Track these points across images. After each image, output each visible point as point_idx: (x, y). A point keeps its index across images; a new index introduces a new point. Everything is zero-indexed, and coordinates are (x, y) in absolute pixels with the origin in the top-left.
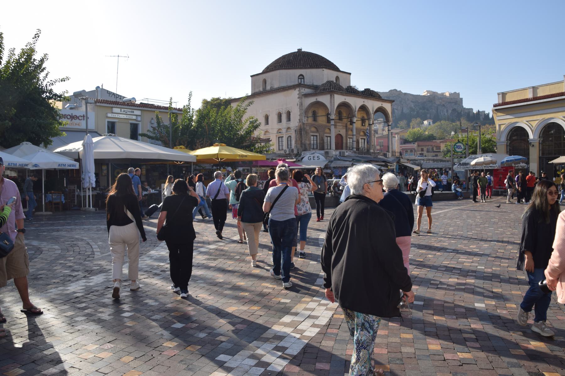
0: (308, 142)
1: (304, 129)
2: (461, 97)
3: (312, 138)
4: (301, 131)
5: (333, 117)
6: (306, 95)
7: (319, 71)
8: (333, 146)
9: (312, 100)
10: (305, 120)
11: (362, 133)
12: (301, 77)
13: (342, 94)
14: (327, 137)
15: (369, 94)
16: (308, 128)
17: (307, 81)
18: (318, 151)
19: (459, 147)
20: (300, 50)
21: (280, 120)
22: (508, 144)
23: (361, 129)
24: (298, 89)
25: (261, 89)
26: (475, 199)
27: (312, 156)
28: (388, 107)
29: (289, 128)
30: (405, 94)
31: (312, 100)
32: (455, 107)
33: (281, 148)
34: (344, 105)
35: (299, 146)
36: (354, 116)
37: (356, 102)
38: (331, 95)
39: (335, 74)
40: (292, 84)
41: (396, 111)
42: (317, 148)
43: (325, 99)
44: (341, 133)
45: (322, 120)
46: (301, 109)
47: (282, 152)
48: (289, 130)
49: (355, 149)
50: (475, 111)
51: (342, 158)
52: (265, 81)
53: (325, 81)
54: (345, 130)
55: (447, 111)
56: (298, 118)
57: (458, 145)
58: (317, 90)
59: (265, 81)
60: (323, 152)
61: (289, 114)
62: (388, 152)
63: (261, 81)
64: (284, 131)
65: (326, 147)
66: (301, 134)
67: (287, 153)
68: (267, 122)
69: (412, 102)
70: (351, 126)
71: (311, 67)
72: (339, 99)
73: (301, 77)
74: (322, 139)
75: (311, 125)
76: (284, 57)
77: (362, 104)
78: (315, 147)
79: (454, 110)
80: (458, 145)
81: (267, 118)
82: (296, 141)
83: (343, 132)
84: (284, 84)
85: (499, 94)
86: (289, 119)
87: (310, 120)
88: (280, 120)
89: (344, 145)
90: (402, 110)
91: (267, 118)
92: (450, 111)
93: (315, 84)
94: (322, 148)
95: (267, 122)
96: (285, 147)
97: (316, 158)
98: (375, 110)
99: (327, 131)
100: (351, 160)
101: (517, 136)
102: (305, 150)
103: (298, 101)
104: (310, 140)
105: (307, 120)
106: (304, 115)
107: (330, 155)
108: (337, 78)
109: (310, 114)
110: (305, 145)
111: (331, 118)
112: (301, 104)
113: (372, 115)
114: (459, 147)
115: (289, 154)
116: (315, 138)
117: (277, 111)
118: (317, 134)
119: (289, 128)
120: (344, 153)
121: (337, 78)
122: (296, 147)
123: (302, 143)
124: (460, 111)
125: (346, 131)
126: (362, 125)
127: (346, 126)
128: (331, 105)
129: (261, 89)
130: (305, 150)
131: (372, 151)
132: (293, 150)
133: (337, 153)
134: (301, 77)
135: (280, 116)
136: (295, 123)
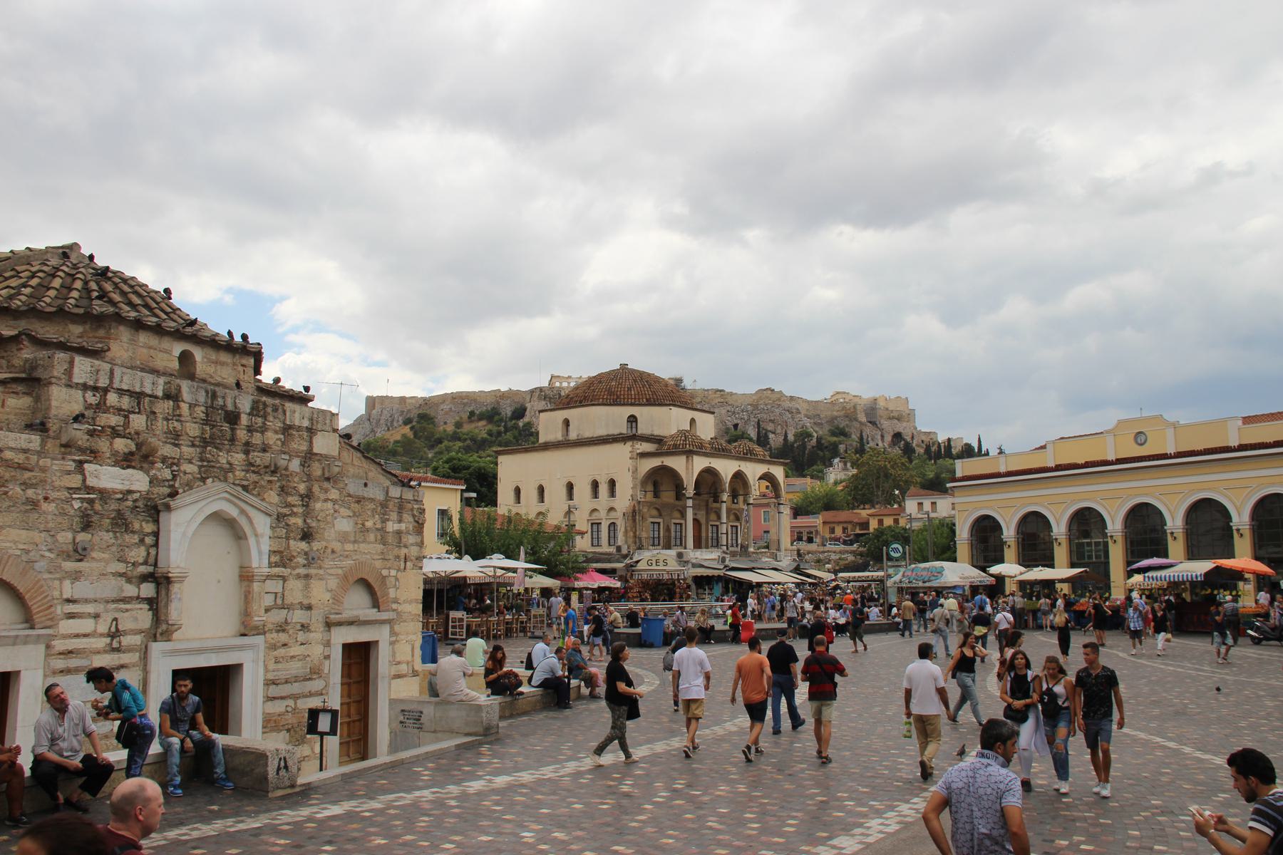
0: (644, 535)
4: (634, 515)
6: (644, 455)
10: (640, 496)
11: (732, 517)
13: (706, 455)
16: (645, 510)
17: (643, 429)
20: (624, 366)
26: (903, 635)
29: (612, 509)
31: (655, 462)
32: (900, 427)
33: (595, 542)
34: (709, 472)
35: (630, 541)
37: (726, 468)
40: (616, 431)
41: (771, 436)
44: (699, 517)
45: (668, 496)
48: (613, 514)
50: (941, 438)
52: (567, 423)
53: (674, 431)
54: (704, 512)
55: (882, 436)
56: (631, 492)
58: (662, 445)
59: (567, 423)
60: (672, 553)
61: (612, 483)
63: (560, 422)
64: (603, 514)
65: (673, 543)
66: (634, 521)
70: (715, 505)
71: (651, 403)
72: (700, 463)
73: (632, 420)
74: (668, 530)
75: (650, 505)
76: (600, 379)
79: (898, 436)
81: (570, 487)
82: (626, 531)
83: (702, 517)
84: (601, 432)
86: (612, 493)
87: (650, 496)
91: (570, 487)
92: (888, 438)
93: (656, 433)
97: (661, 563)
99: (677, 514)
101: (986, 529)
102: (640, 548)
103: (630, 463)
106: (639, 487)
108: (693, 421)
109: (650, 487)
112: (635, 471)
114: (896, 550)
117: (590, 480)
118: (660, 520)
121: (693, 421)
123: (635, 536)
124: (909, 439)
125: (707, 513)
127: (707, 505)
129: (559, 436)
132: (619, 549)
134: (632, 420)
135: (595, 485)
136: (623, 501)
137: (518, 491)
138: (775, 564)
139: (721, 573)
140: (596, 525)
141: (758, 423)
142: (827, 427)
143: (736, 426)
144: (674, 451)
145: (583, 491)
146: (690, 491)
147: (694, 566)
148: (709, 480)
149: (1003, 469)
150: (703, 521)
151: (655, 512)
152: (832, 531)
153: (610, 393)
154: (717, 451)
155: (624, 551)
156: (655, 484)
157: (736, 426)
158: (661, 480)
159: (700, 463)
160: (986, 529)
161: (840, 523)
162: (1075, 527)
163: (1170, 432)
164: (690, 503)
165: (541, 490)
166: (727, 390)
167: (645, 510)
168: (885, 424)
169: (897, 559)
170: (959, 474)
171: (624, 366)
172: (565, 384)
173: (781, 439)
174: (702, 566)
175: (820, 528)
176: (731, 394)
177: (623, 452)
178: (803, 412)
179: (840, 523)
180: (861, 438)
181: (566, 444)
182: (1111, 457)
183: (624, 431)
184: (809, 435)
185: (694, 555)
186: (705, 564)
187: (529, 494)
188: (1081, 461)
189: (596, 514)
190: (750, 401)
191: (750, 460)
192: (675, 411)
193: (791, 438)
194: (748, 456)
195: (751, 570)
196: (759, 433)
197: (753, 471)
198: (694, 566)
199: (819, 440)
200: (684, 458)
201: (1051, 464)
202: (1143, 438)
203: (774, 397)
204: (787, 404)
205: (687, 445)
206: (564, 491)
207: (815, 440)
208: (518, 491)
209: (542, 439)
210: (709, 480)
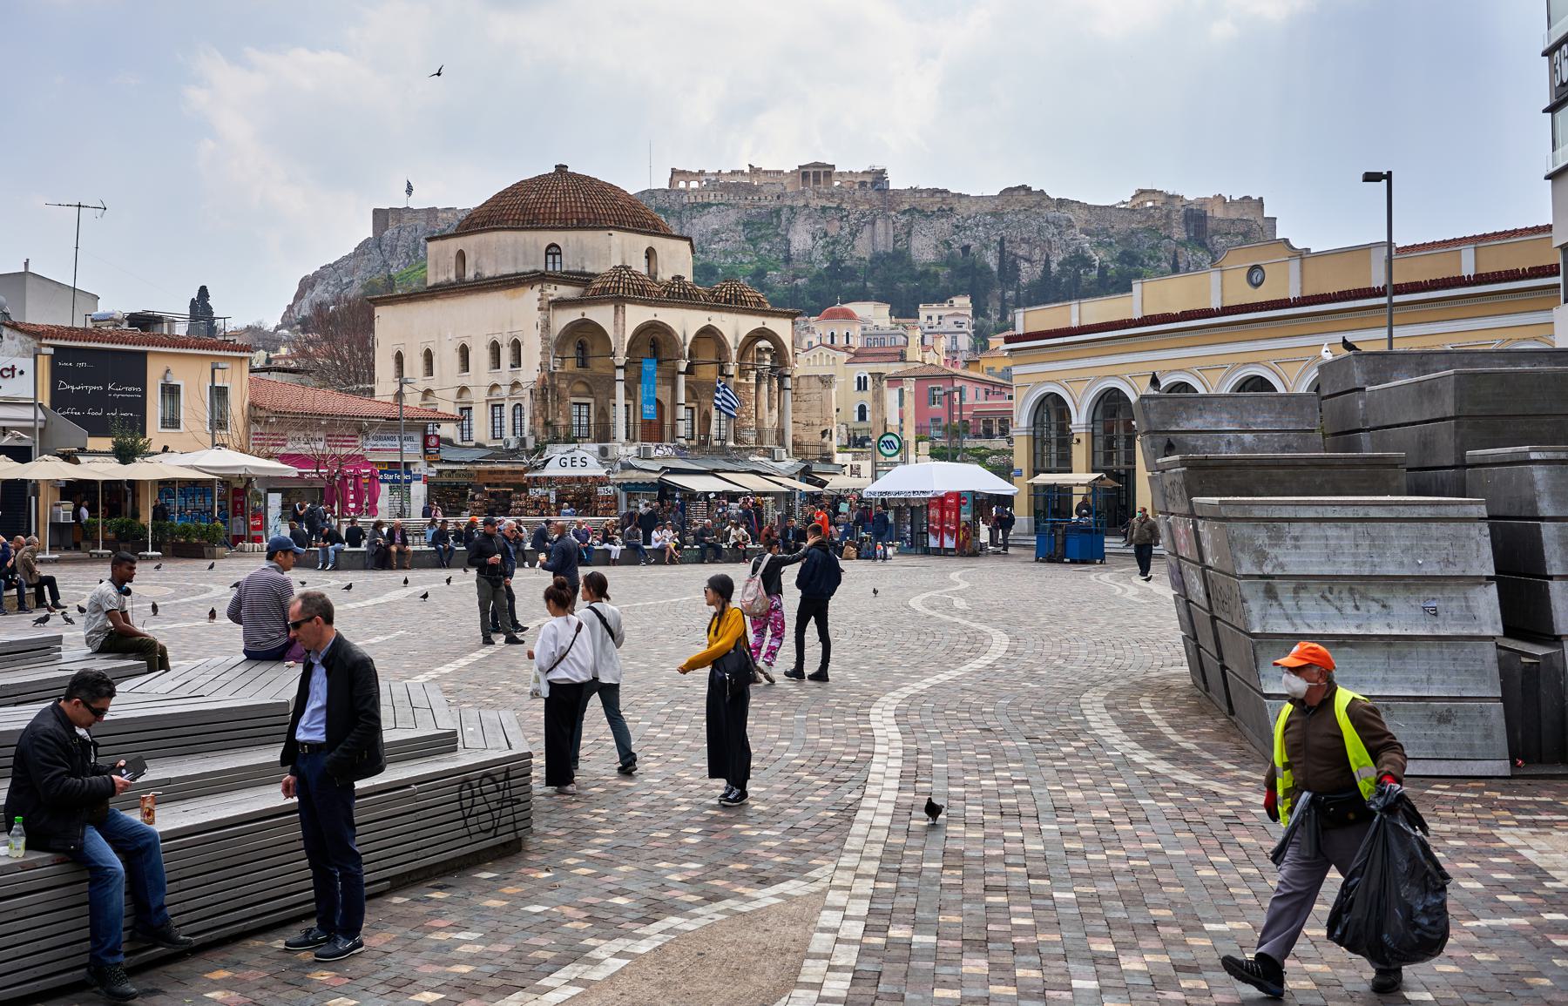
0: (562, 421)
1: (554, 387)
3: (575, 409)
4: (546, 392)
6: (560, 304)
7: (602, 234)
8: (620, 432)
9: (574, 315)
12: (554, 250)
16: (563, 385)
17: (569, 263)
18: (583, 447)
20: (561, 168)
21: (496, 363)
24: (538, 287)
25: (452, 277)
27: (569, 456)
29: (516, 385)
30: (1061, 203)
31: (574, 315)
33: (497, 434)
35: (539, 430)
36: (681, 356)
37: (685, 323)
39: (645, 241)
41: (1024, 265)
43: (602, 315)
46: (545, 339)
47: (500, 443)
51: (639, 463)
52: (461, 256)
56: (539, 359)
59: (461, 256)
60: (595, 447)
61: (516, 346)
63: (453, 254)
64: (505, 391)
66: (545, 401)
67: (511, 447)
68: (465, 365)
69: (1083, 231)
71: (581, 226)
72: (638, 315)
73: (553, 250)
75: (572, 378)
78: (584, 432)
81: (464, 352)
82: (533, 419)
84: (508, 269)
86: (517, 362)
87: (570, 365)
88: (496, 363)
89: (667, 430)
90: (1048, 263)
91: (464, 352)
93: (588, 270)
94: (598, 440)
95: (465, 365)
96: (508, 433)
97: (579, 463)
98: (741, 339)
103: (538, 316)
104: (569, 416)
105: (562, 365)
108: (650, 254)
109: (571, 351)
110: (555, 428)
112: (547, 326)
113: (734, 354)
115: (517, 450)
116: (584, 409)
119: (516, 385)
120: (647, 450)
121: (650, 254)
122: (533, 432)
123: (547, 424)
129: (452, 277)
130: (556, 440)
132: (523, 441)
133: (633, 449)
134: (553, 250)
135: (495, 349)
136: (530, 373)
137: (399, 358)
140: (496, 407)
141: (1001, 243)
143: (966, 249)
145: (480, 356)
146: (621, 359)
148: (653, 340)
149: (1075, 323)
150: (667, 402)
151: (580, 388)
153: (525, 210)
154: (677, 295)
155: (530, 445)
156: (582, 348)
157: (966, 249)
158: (583, 342)
163: (1295, 264)
164: (620, 374)
165: (428, 356)
167: (563, 385)
170: (1020, 331)
171: (561, 168)
172: (694, 185)
173: (1039, 269)
177: (530, 297)
181: (460, 287)
182: (1215, 304)
183: (542, 268)
187: (414, 365)
188: (1177, 310)
189: (497, 391)
190: (989, 207)
191: (730, 310)
192: (617, 236)
193: (1054, 267)
194: (734, 303)
195: (713, 473)
197: (734, 327)
201: (1137, 316)
202: (1256, 276)
203: (1031, 200)
204: (1051, 213)
205: (623, 288)
206: (456, 358)
208: (399, 358)
209: (430, 282)
210: (653, 340)
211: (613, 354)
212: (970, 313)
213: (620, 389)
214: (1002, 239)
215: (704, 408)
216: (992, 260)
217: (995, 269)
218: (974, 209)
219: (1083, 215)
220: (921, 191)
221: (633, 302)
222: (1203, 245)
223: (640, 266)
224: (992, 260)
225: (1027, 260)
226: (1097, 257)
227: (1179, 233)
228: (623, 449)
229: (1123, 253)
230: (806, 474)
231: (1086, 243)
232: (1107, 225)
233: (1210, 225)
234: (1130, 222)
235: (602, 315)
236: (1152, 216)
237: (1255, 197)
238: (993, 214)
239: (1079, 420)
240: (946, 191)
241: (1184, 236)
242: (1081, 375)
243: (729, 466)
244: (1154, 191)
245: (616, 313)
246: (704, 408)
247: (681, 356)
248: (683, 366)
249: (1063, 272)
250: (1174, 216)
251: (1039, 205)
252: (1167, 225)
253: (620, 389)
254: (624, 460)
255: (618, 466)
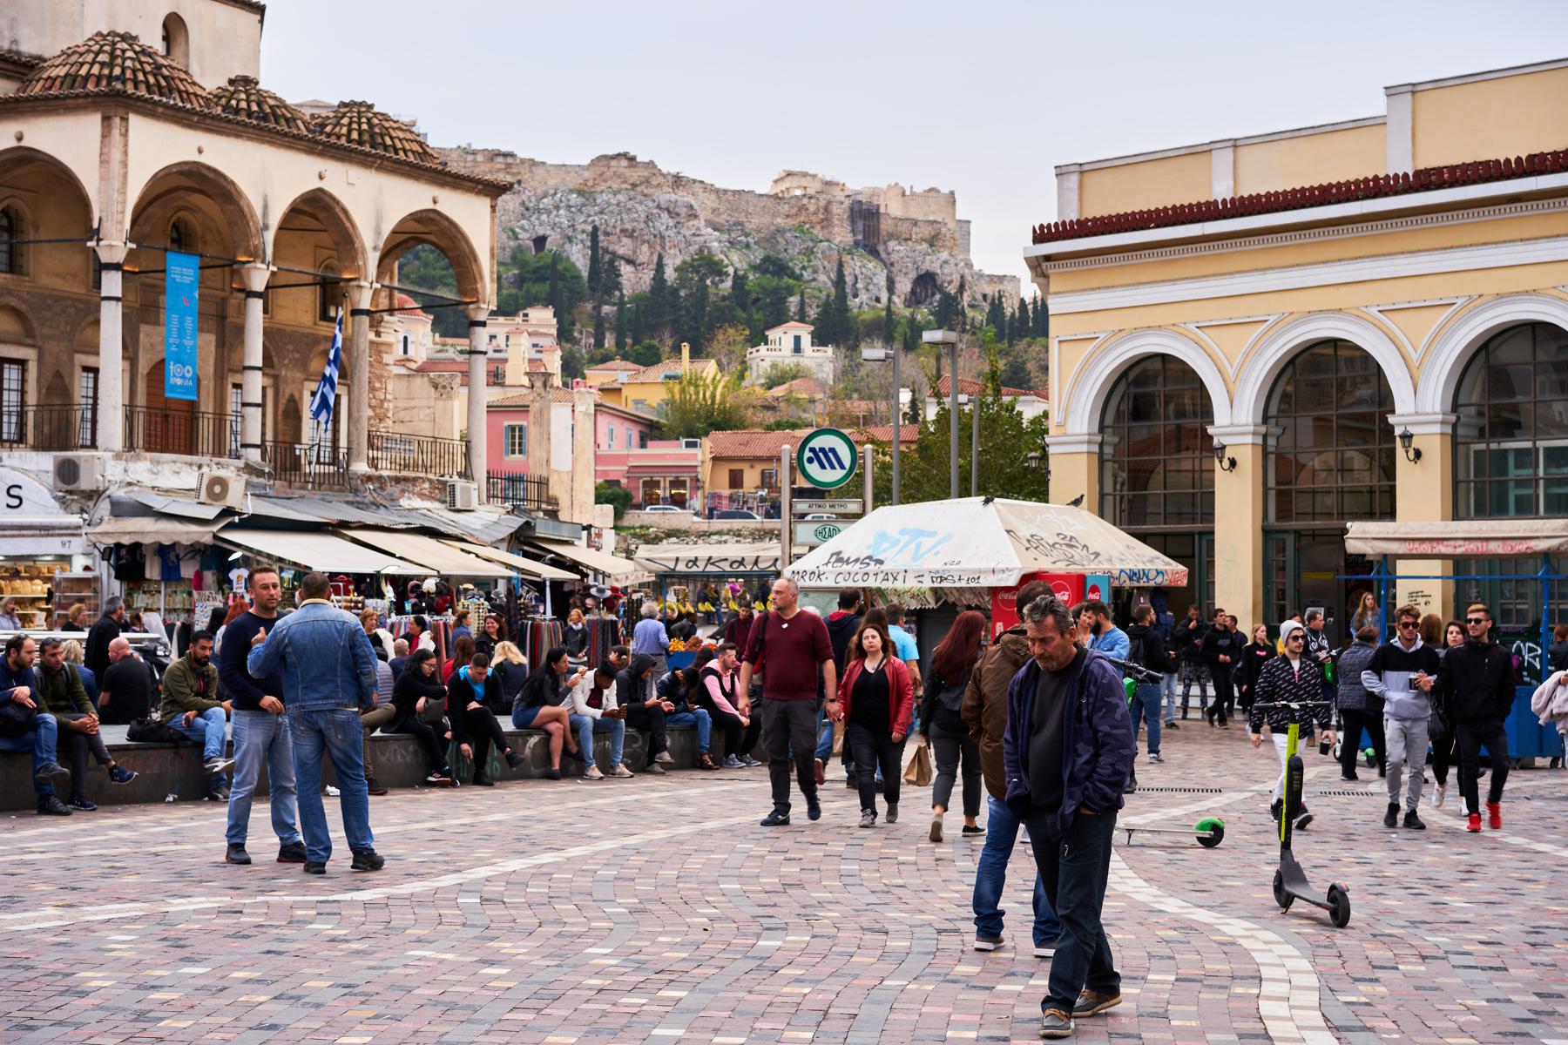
2: (961, 214)
5: (115, 244)
14: (86, 369)
15: (364, 138)
19: (826, 457)
22: (1108, 450)
23: (315, 340)
28: (472, 218)
30: (678, 181)
32: (931, 263)
36: (257, 254)
37: (269, 179)
38: (106, 119)
41: (626, 270)
42: (21, 439)
43: (68, 140)
49: (254, 455)
53: (81, 35)
57: (816, 443)
60: (46, 461)
62: (466, 475)
69: (709, 223)
72: (155, 146)
74: (57, 389)
77: (317, 184)
79: (926, 282)
80: (816, 443)
85: (1061, 172)
89: (206, 428)
90: (660, 267)
92: (904, 286)
93: (29, 46)
98: (387, 229)
100: (210, 512)
107: (85, 484)
111: (105, 257)
113: (372, 259)
114: (826, 457)
124: (952, 290)
126: (325, 316)
128: (104, 178)
131: (361, 467)
138: (438, 514)
139: (204, 535)
142: (757, 256)
143: (540, 241)
144: (67, 96)
146: (115, 244)
147: (120, 510)
149: (1222, 191)
152: (736, 480)
157: (540, 241)
159: (155, 146)
160: (1155, 408)
161: (754, 460)
162: (1473, 395)
164: (112, 284)
166: (522, 154)
168: (897, 249)
169: (817, 492)
173: (647, 276)
174: (145, 511)
175: (705, 473)
176: (533, 163)
178: (703, 215)
179: (754, 460)
180: (840, 281)
184: (716, 269)
185: (113, 465)
186: (159, 503)
190: (574, 181)
193: (670, 274)
196: (595, 260)
198: (120, 510)
199: (739, 281)
200: (93, 122)
201: (1400, 164)
203: (635, 175)
204: (665, 196)
207: (728, 283)
211: (95, 234)
212: (554, 331)
213: (111, 320)
214: (595, 229)
215: (287, 390)
216: (579, 257)
217: (585, 274)
218: (552, 182)
219: (710, 201)
220: (474, 153)
221: (149, 109)
222: (874, 253)
223: (153, 39)
224: (579, 257)
225: (630, 262)
226: (736, 262)
227: (842, 234)
228: (113, 465)
229: (766, 259)
230: (523, 541)
231: (715, 243)
232: (742, 218)
233: (886, 226)
234: (774, 215)
235: (68, 140)
236: (803, 208)
237: (945, 190)
238: (580, 192)
239: (1236, 416)
240: (512, 155)
241: (849, 239)
242: (1240, 311)
243: (369, 517)
244: (805, 175)
245: (106, 133)
246: (287, 390)
247: (257, 254)
248: (259, 278)
249: (682, 281)
250: (835, 209)
251: (647, 181)
252: (826, 222)
253: (111, 320)
254: (120, 493)
255: (104, 507)
